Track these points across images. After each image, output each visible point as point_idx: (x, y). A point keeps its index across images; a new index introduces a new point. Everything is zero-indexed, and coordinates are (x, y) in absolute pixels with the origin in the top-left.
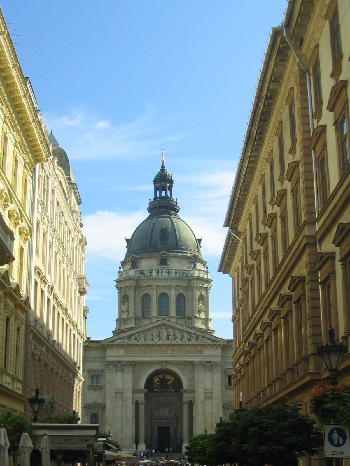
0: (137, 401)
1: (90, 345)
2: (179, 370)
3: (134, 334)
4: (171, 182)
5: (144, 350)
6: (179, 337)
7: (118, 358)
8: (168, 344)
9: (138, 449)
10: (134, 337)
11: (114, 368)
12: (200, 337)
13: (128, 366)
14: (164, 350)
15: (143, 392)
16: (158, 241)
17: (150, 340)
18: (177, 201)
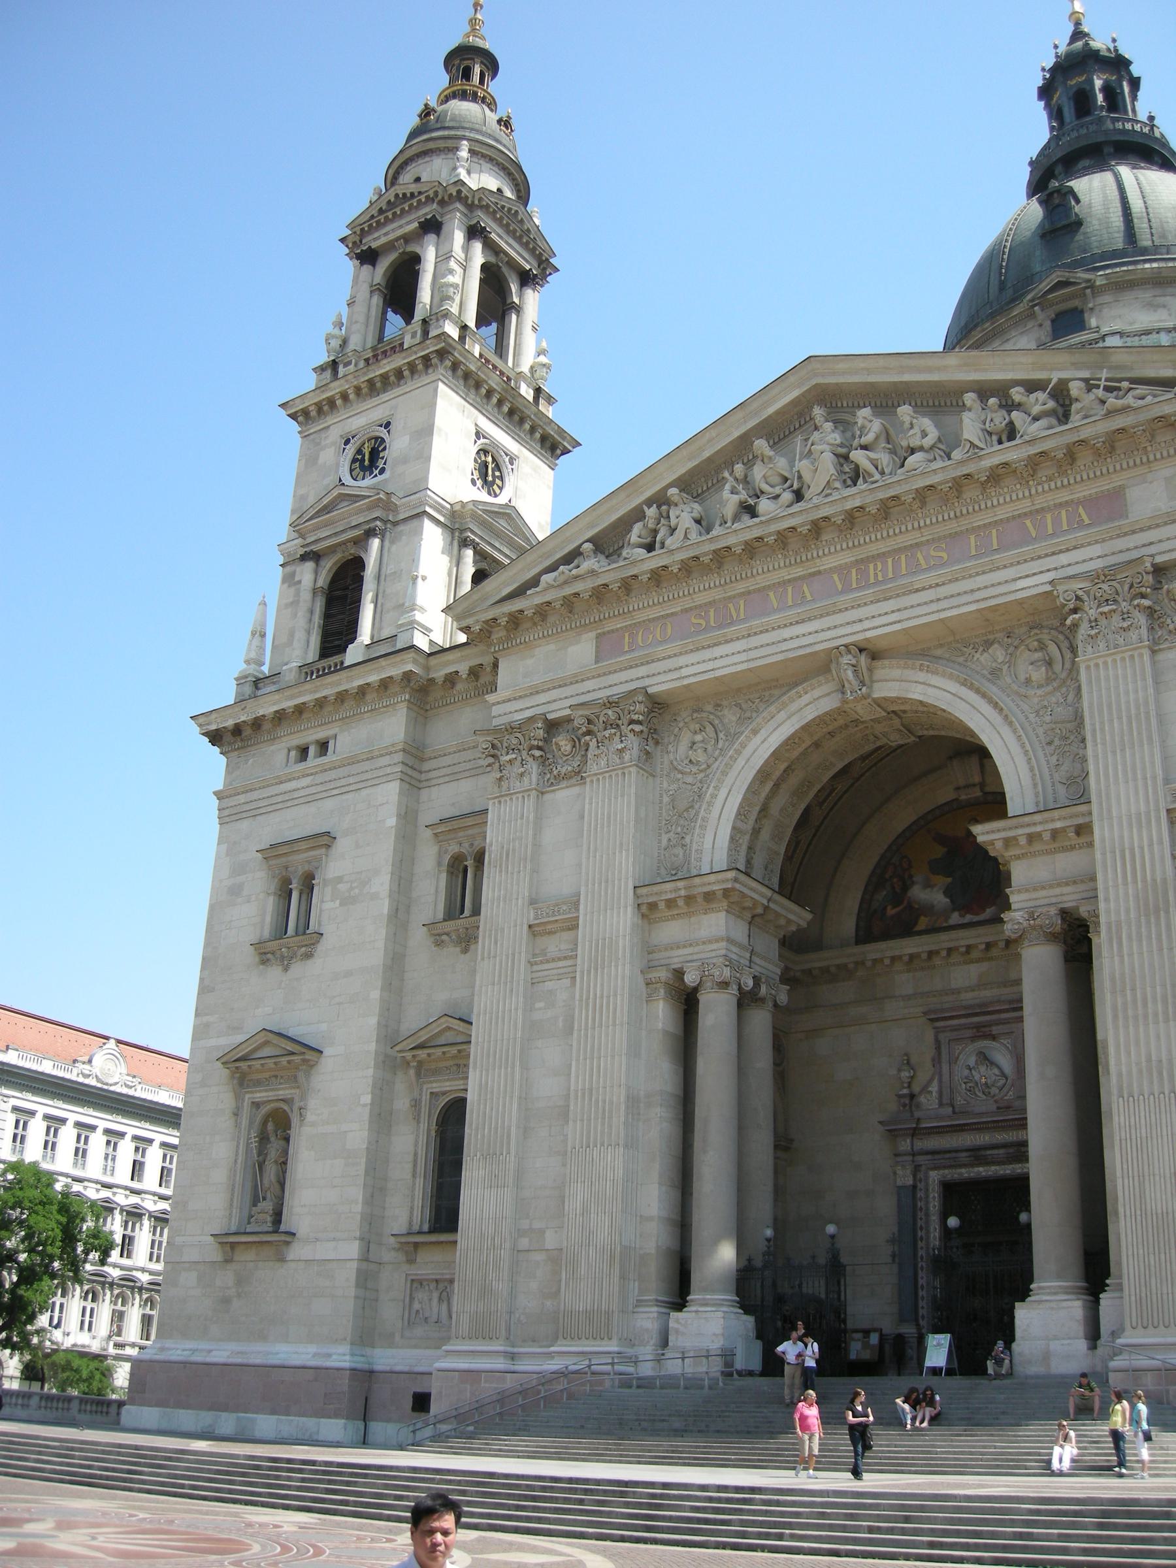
0: (679, 974)
1: (439, 674)
2: (964, 692)
3: (637, 515)
4: (1118, 64)
5: (711, 604)
6: (928, 442)
7: (554, 694)
8: (849, 505)
9: (672, 1339)
10: (636, 533)
11: (534, 768)
12: (1075, 389)
13: (607, 733)
14: (839, 569)
15: (709, 897)
16: (1038, 253)
17: (736, 518)
18: (1155, 122)
